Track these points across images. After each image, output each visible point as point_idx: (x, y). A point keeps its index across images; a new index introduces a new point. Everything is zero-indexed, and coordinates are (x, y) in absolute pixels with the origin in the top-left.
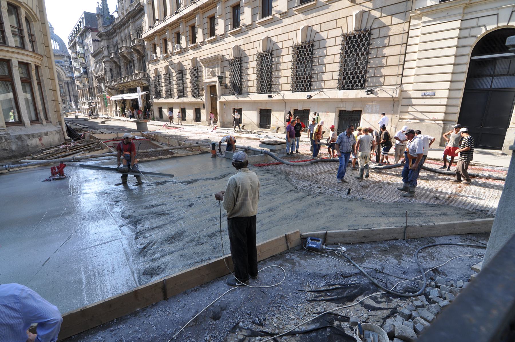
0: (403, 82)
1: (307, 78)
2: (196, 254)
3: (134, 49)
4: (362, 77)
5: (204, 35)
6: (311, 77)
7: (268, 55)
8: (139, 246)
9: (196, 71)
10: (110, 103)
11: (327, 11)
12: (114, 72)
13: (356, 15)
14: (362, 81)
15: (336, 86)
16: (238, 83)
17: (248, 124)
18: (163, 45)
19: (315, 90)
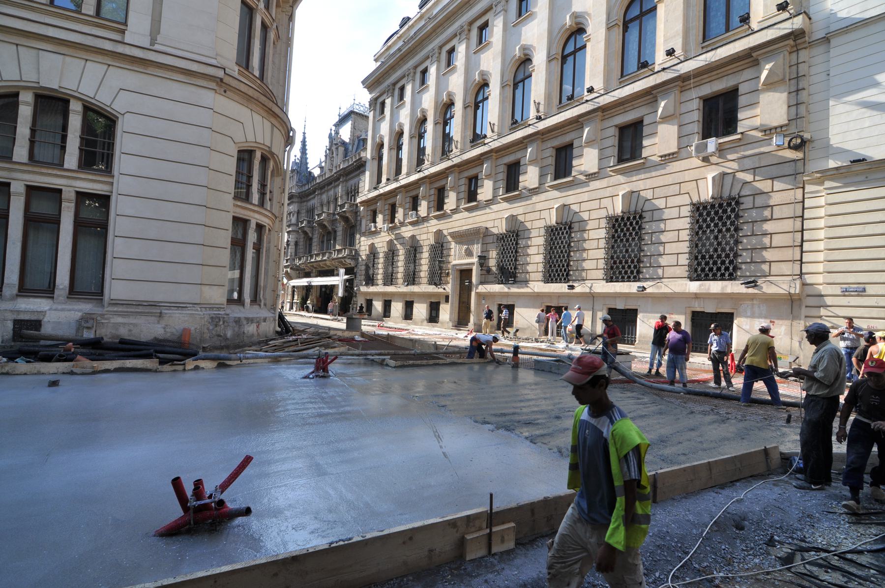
0: (804, 271)
1: (632, 262)
3: (341, 216)
4: (731, 262)
5: (458, 200)
6: (639, 261)
7: (565, 228)
9: (439, 249)
10: (284, 289)
11: (663, 172)
13: (714, 178)
14: (731, 268)
15: (686, 274)
16: (510, 268)
17: (524, 329)
19: (646, 279)
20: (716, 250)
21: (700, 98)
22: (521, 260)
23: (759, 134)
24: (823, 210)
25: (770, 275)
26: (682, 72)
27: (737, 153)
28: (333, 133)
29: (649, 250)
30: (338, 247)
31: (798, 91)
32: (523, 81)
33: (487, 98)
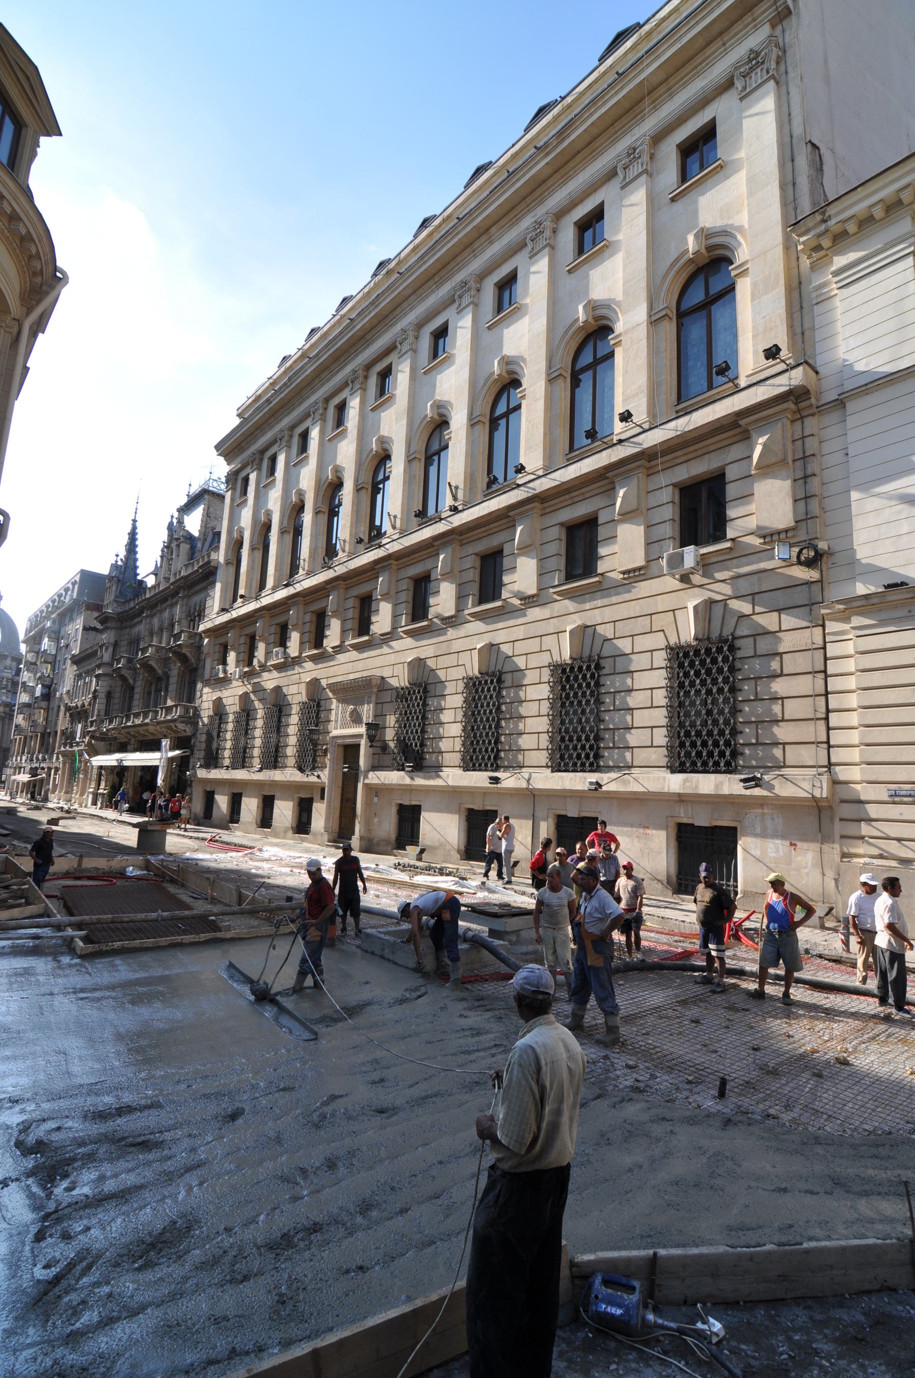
0: (833, 760)
1: (587, 739)
2: (217, 1322)
3: (175, 653)
4: (727, 744)
5: (344, 632)
6: (598, 738)
7: (492, 682)
8: (40, 1273)
9: (315, 708)
11: (627, 596)
12: (116, 699)
14: (728, 753)
15: (664, 761)
16: (415, 744)
17: (434, 848)
19: (609, 769)
21: (674, 485)
22: (431, 732)
23: (756, 541)
24: (852, 660)
25: (785, 766)
26: (645, 446)
28: (175, 521)
29: (612, 720)
30: (170, 703)
31: (805, 477)
32: (438, 453)
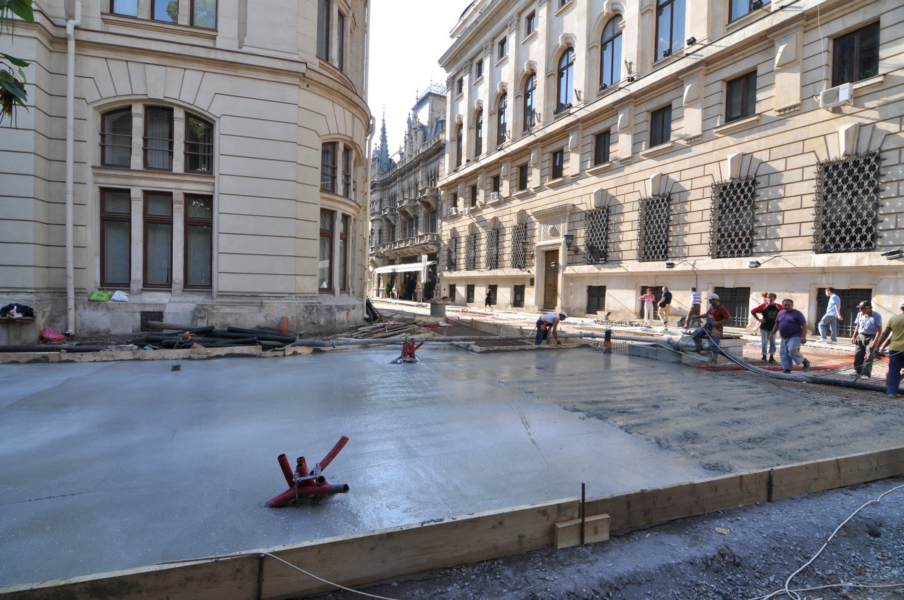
1: (744, 234)
3: (422, 202)
4: (869, 230)
5: (542, 177)
6: (752, 233)
7: (663, 201)
9: (523, 230)
10: (370, 277)
11: (782, 128)
12: (385, 234)
13: (847, 132)
15: (811, 246)
16: (601, 247)
17: (616, 312)
18: (469, 195)
19: (761, 254)
20: (849, 216)
21: (829, 37)
26: (806, 9)
27: (878, 99)
28: (411, 117)
32: (612, 40)
33: (572, 64)
